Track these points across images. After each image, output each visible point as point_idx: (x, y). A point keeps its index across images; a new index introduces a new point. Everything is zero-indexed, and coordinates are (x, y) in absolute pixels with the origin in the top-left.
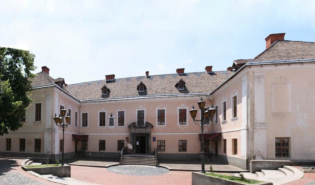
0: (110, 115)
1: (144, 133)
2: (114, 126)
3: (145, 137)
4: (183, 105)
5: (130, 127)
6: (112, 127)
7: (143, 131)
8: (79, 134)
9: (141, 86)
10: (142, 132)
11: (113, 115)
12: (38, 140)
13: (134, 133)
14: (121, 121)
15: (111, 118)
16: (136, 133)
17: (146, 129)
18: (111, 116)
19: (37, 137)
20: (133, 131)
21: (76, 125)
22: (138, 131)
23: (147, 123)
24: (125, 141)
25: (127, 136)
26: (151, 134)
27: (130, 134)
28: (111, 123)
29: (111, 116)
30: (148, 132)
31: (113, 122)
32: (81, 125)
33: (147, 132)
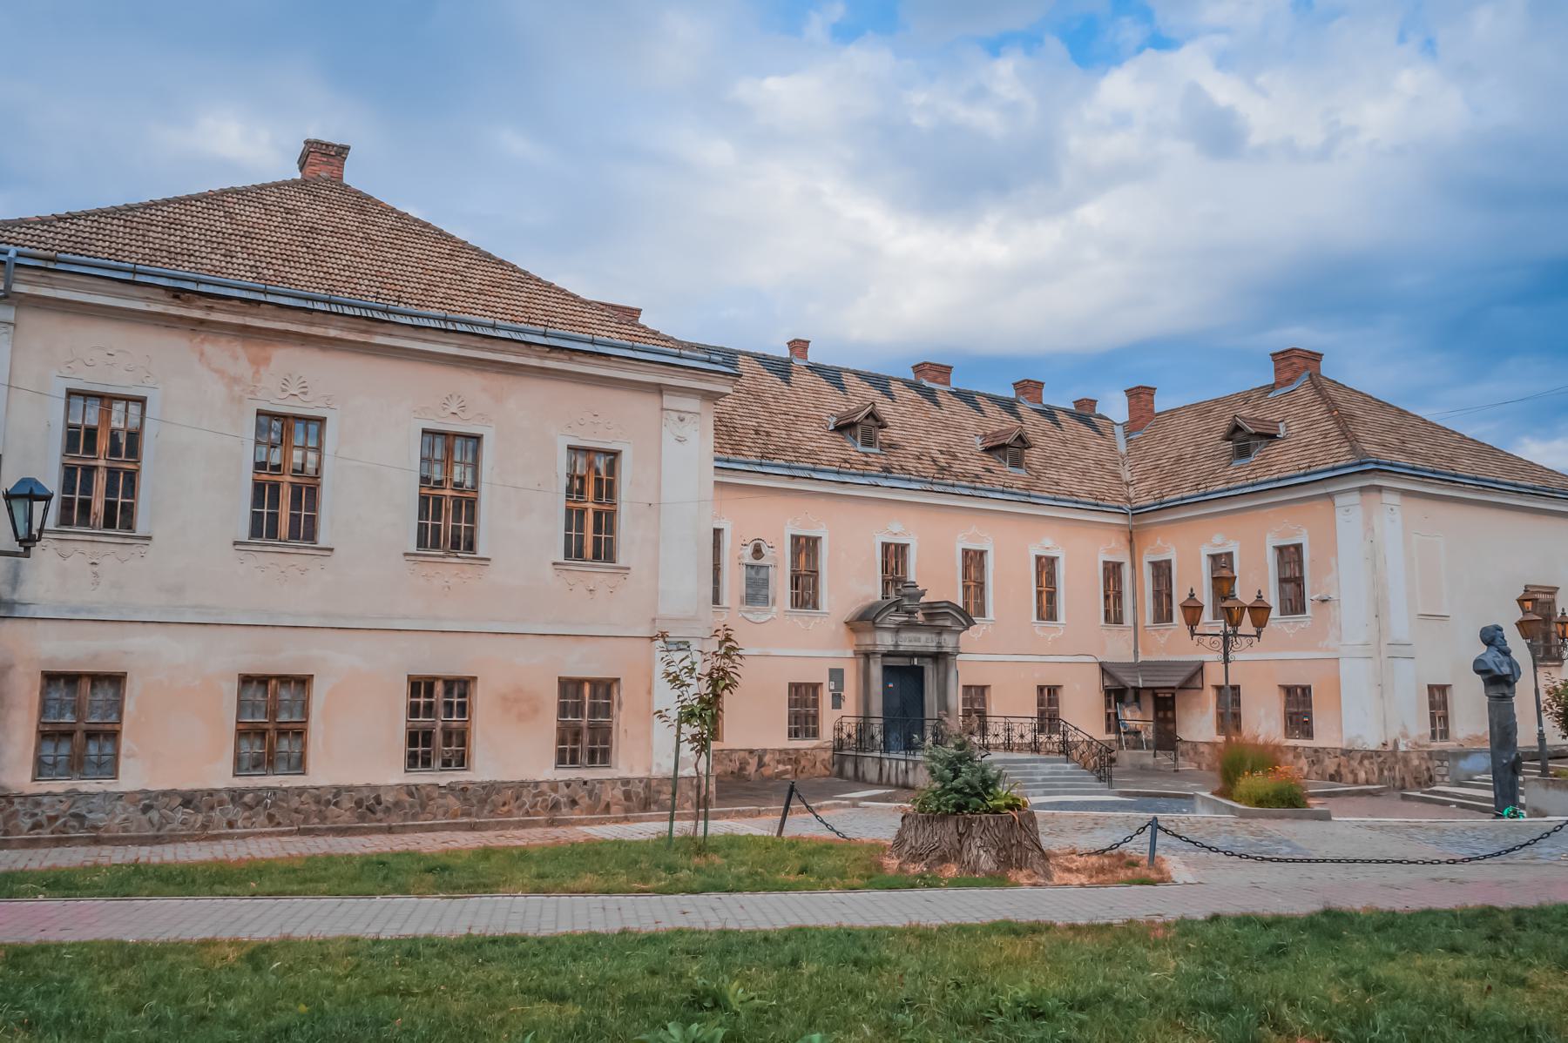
0: (749, 550)
2: (775, 609)
3: (918, 673)
4: (1048, 543)
6: (759, 615)
7: (923, 641)
11: (764, 549)
12: (587, 688)
14: (805, 591)
15: (752, 567)
17: (940, 634)
18: (757, 552)
19: (586, 664)
20: (885, 641)
24: (825, 688)
25: (837, 665)
26: (959, 657)
28: (757, 591)
29: (757, 552)
31: (766, 583)
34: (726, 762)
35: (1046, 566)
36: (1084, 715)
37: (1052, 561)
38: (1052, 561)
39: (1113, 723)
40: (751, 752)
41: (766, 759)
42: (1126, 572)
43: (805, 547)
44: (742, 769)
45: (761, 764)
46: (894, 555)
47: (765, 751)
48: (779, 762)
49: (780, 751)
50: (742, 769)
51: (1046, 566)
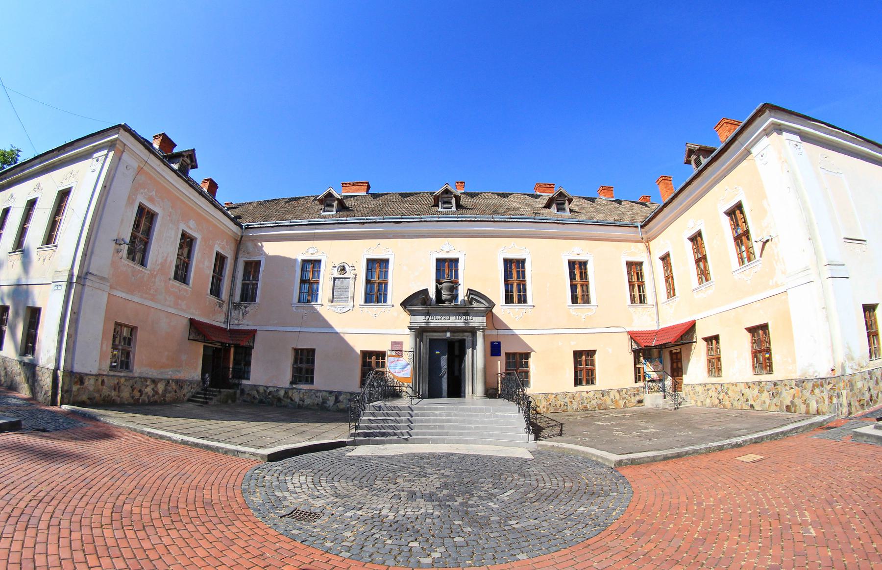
1: (459, 325)
5: (406, 304)
8: (224, 326)
9: (445, 196)
10: (453, 325)
11: (347, 268)
13: (423, 325)
16: (432, 325)
18: (343, 269)
20: (420, 320)
21: (216, 291)
22: (436, 321)
23: (471, 292)
27: (410, 329)
30: (476, 325)
32: (237, 299)
33: (471, 325)
34: (313, 397)
35: (578, 268)
36: (615, 370)
37: (583, 264)
38: (583, 264)
39: (639, 375)
40: (331, 392)
41: (341, 398)
42: (646, 268)
43: (377, 267)
44: (324, 402)
45: (337, 401)
46: (446, 267)
47: (340, 393)
48: (350, 400)
49: (351, 394)
50: (324, 402)
51: (578, 268)
